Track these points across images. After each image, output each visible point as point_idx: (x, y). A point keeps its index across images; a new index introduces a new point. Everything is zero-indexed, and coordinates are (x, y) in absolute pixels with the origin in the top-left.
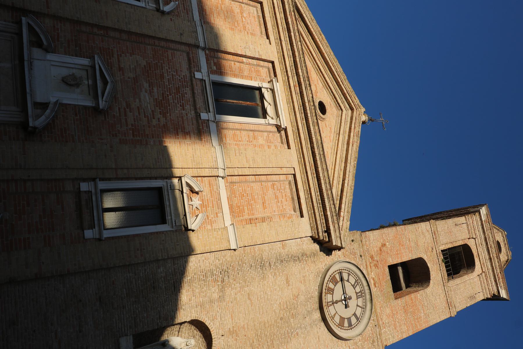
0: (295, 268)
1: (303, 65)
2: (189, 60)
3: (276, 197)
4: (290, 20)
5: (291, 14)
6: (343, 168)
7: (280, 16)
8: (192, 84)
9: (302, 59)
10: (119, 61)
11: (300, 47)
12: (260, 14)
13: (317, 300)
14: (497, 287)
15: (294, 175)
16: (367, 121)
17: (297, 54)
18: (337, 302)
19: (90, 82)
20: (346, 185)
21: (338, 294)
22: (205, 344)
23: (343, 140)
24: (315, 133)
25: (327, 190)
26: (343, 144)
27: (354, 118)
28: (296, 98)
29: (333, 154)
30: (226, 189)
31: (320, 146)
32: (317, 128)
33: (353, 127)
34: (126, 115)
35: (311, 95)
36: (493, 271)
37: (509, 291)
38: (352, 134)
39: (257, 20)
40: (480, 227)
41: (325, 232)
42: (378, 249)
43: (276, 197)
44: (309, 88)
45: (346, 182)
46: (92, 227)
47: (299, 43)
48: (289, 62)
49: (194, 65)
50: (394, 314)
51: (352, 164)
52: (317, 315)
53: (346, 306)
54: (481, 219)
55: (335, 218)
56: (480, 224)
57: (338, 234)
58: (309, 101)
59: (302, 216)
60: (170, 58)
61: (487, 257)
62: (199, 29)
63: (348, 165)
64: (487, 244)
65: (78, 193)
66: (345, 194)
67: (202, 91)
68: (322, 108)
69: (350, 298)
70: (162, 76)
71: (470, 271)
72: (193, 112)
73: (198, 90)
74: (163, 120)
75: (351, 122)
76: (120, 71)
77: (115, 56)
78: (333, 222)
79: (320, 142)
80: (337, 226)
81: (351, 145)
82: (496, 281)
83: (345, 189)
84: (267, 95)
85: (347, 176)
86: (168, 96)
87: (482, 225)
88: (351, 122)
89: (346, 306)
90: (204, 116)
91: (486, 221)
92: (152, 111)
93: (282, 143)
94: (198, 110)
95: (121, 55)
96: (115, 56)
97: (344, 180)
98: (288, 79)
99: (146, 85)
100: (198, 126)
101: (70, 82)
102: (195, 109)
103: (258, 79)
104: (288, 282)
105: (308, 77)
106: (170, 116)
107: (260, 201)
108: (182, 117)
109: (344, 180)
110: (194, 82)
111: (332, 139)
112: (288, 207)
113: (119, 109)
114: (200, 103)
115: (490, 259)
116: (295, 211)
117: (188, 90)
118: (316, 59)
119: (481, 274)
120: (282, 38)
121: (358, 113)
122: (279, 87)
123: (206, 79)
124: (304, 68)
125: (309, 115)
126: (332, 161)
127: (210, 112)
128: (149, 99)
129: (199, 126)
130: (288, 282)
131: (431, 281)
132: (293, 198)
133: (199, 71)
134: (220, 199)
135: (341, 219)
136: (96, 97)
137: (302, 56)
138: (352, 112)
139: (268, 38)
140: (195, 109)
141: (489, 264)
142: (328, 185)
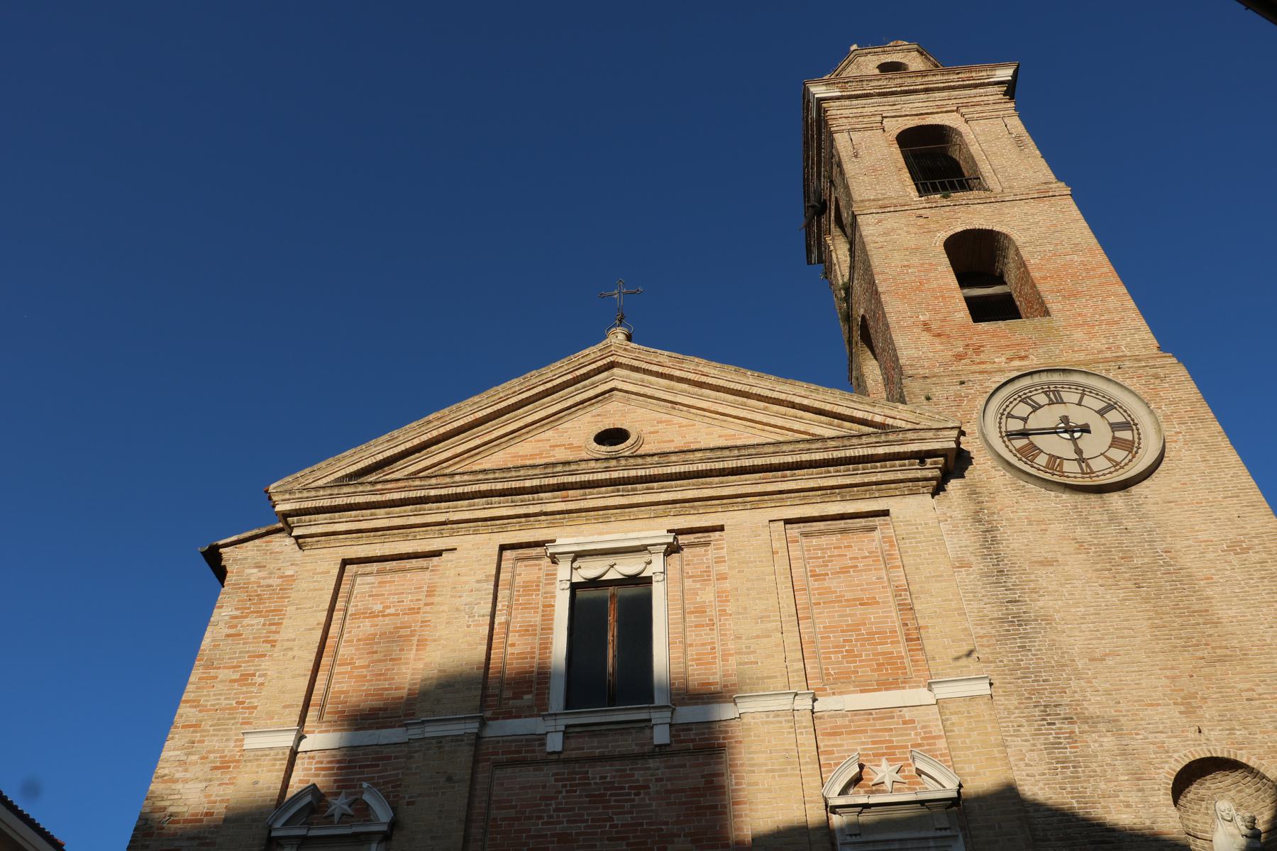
0: (1014, 542)
1: (514, 474)
2: (513, 763)
3: (844, 570)
4: (396, 496)
5: (381, 492)
6: (762, 404)
7: (382, 519)
8: (577, 760)
9: (497, 475)
11: (466, 477)
12: (375, 567)
13: (1080, 497)
14: (989, 84)
15: (788, 522)
17: (484, 487)
18: (1079, 451)
20: (806, 402)
21: (1058, 446)
22: (1219, 775)
23: (690, 395)
24: (685, 462)
25: (826, 449)
26: (700, 397)
27: (636, 363)
28: (595, 499)
29: (724, 424)
30: (841, 693)
31: (719, 454)
32: (673, 458)
33: (660, 369)
35: (592, 464)
36: (953, 88)
37: (998, 60)
38: (677, 373)
39: (388, 578)
40: (855, 102)
41: (922, 462)
42: (937, 340)
43: (844, 570)
44: (573, 467)
45: (798, 400)
47: (457, 478)
48: (502, 508)
49: (527, 752)
50: (1085, 323)
51: (751, 381)
52: (1115, 499)
53: (1085, 429)
54: (838, 98)
55: (891, 437)
56: (847, 102)
57: (930, 434)
58: (607, 469)
59: (885, 513)
60: (512, 813)
61: (922, 96)
62: (432, 731)
63: (754, 390)
64: (893, 93)
66: (828, 407)
67: (594, 734)
68: (613, 436)
69: (1065, 419)
71: (956, 139)
72: (652, 763)
73: (593, 746)
75: (646, 372)
78: (902, 442)
79: (709, 454)
80: (910, 435)
81: (704, 379)
82: (976, 86)
83: (817, 405)
84: (590, 570)
85: (783, 397)
86: (616, 826)
87: (850, 97)
88: (646, 372)
89: (1085, 429)
90: (661, 736)
91: (843, 89)
93: (707, 544)
94: (646, 749)
97: (793, 405)
98: (546, 514)
102: (643, 756)
103: (549, 588)
104: (1046, 563)
105: (546, 465)
106: (666, 823)
107: (859, 610)
108: (667, 791)
109: (793, 405)
110: (574, 754)
111: (685, 422)
112: (864, 544)
114: (628, 744)
115: (926, 90)
116: (873, 529)
118: (486, 438)
119: (963, 115)
120: (442, 518)
121: (621, 352)
122: (568, 538)
123: (562, 723)
124: (522, 473)
125: (641, 473)
126: (742, 428)
127: (650, 720)
130: (1046, 563)
131: (997, 229)
132: (843, 531)
133: (541, 739)
134: (868, 712)
135: (889, 421)
137: (491, 476)
138: (620, 365)
139: (438, 553)
140: (643, 756)
141: (937, 95)
142: (814, 446)
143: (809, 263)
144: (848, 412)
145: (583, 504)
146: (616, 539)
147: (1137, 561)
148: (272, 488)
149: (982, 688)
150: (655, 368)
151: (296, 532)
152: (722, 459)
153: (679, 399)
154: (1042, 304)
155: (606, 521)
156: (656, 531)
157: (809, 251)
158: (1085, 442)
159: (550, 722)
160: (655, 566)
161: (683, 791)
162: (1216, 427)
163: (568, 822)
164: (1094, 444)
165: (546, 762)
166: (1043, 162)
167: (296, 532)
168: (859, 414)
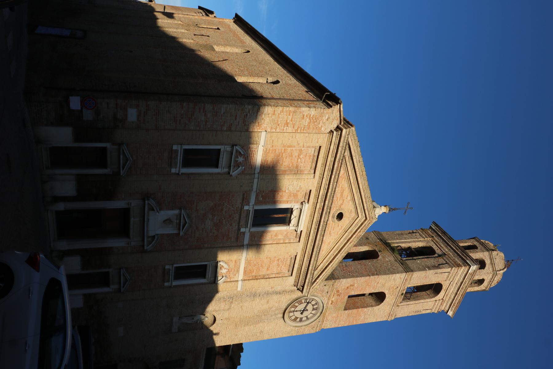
0: (275, 297)
2: (243, 198)
3: (278, 265)
4: (336, 166)
5: (339, 161)
6: (335, 254)
13: (284, 310)
16: (387, 212)
17: (330, 190)
18: (296, 311)
20: (330, 266)
21: (301, 307)
23: (347, 236)
26: (345, 239)
28: (317, 215)
35: (327, 219)
37: (456, 314)
38: (354, 236)
40: (464, 275)
42: (346, 287)
43: (278, 265)
45: (331, 264)
46: (168, 281)
47: (335, 184)
50: (338, 316)
51: (343, 254)
52: (282, 315)
53: (302, 313)
54: (468, 271)
56: (465, 273)
58: (324, 222)
61: (455, 292)
62: (256, 181)
63: (339, 254)
64: (461, 285)
65: (164, 269)
66: (326, 270)
67: (247, 216)
68: (340, 216)
69: (307, 310)
70: (222, 210)
71: (432, 295)
72: (237, 227)
73: (243, 215)
80: (309, 287)
81: (349, 242)
82: (450, 305)
83: (328, 268)
84: (295, 213)
85: (334, 261)
90: (242, 230)
91: (470, 274)
93: (296, 237)
97: (331, 262)
99: (210, 216)
100: (238, 234)
101: (168, 221)
102: (239, 225)
103: (293, 202)
104: (268, 302)
105: (331, 208)
107: (266, 267)
109: (331, 262)
110: (243, 212)
114: (243, 222)
115: (456, 294)
117: (237, 217)
119: (439, 300)
120: (325, 176)
122: (307, 208)
123: (251, 210)
125: (320, 229)
129: (238, 234)
130: (268, 302)
135: (316, 283)
136: (179, 229)
139: (314, 173)
140: (239, 225)
143: (434, 223)
144: (323, 274)
145: (317, 212)
146: (303, 219)
147: (263, 317)
148: (353, 128)
149: (239, 289)
150: (359, 230)
151: (335, 133)
152: (317, 248)
154: (349, 309)
155: (311, 216)
156: (303, 226)
157: (436, 225)
158: (300, 313)
159: (252, 207)
160: (292, 227)
162: (294, 335)
164: (298, 314)
165: (242, 205)
166: (406, 315)
167: (335, 133)
168: (321, 277)
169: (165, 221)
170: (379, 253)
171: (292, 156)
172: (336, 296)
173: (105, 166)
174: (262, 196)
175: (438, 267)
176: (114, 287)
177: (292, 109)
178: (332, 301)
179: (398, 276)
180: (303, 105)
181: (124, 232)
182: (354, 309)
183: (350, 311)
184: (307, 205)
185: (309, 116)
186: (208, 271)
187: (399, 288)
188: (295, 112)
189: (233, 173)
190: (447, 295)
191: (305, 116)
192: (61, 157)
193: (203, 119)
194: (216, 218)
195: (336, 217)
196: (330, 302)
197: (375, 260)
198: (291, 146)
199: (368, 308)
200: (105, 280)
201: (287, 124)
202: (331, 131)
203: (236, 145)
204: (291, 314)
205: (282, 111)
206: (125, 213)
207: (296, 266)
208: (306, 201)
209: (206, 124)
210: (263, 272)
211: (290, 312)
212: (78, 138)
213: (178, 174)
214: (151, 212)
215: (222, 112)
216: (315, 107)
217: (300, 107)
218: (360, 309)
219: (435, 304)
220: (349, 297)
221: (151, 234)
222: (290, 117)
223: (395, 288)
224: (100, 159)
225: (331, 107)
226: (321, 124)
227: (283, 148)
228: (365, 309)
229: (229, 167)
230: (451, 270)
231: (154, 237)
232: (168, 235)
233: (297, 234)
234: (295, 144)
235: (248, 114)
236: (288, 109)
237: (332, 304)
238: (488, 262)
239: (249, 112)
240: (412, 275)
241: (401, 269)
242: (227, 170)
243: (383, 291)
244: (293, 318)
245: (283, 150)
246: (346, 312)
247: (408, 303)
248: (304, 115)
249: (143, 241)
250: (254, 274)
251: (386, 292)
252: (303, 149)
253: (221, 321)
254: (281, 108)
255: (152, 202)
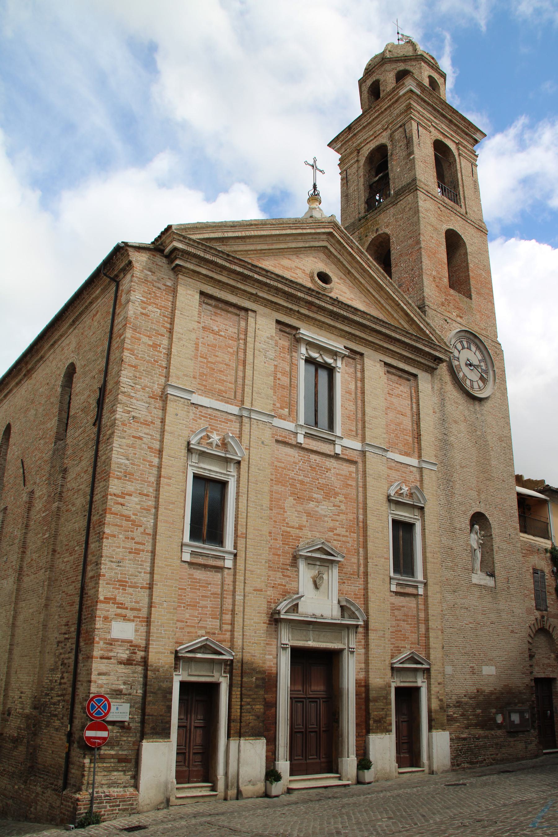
1: (294, 285)
10: (293, 527)
12: (213, 302)
19: (318, 563)
23: (358, 272)
25: (411, 339)
29: (366, 295)
30: (394, 452)
34: (339, 535)
41: (435, 360)
46: (416, 587)
49: (289, 439)
60: (282, 465)
68: (324, 278)
70: (302, 482)
74: (341, 498)
76: (302, 529)
77: (288, 529)
80: (438, 348)
86: (319, 483)
92: (334, 506)
95: (287, 523)
96: (288, 529)
99: (312, 505)
106: (336, 487)
108: (337, 474)
113: (334, 540)
116: (409, 380)
122: (307, 332)
126: (373, 302)
127: (334, 441)
128: (324, 505)
130: (456, 422)
131: (462, 236)
132: (400, 377)
136: (332, 562)
142: (408, 335)
145: (315, 316)
147: (478, 433)
151: (178, 262)
153: (353, 271)
154: (469, 290)
161: (342, 475)
163: (304, 476)
169: (316, 587)
170: (380, 232)
171: (214, 346)
172: (449, 309)
173: (215, 686)
174: (282, 408)
175: (409, 142)
176: (421, 682)
177: (129, 333)
178: (457, 316)
179: (421, 203)
180: (123, 313)
181: (330, 660)
182: (469, 284)
183: (473, 290)
184: (302, 331)
185: (145, 305)
186: (402, 519)
187: (440, 205)
188: (135, 329)
189: (239, 455)
190: (452, 136)
191: (144, 311)
192: (197, 762)
193: (136, 499)
194: (315, 496)
195: (324, 285)
196: (459, 319)
197: (393, 239)
198: (197, 344)
199: (469, 261)
200: (408, 697)
201: (155, 346)
202: (173, 269)
203: (189, 443)
204: (476, 386)
205: (132, 351)
206: (299, 655)
207: (401, 365)
208: (294, 332)
209: (148, 496)
210: (407, 423)
211: (472, 387)
212: (163, 732)
213: (235, 555)
214: (300, 609)
215: (127, 462)
216: (129, 292)
217: (126, 318)
218: (471, 274)
219: (464, 157)
220: (452, 286)
221: (336, 612)
222: (145, 339)
223: (439, 212)
224: (200, 696)
225: (130, 262)
226: (160, 285)
227: (199, 359)
228: (471, 266)
229: (227, 461)
230: (415, 121)
231: (342, 607)
232: (342, 582)
233: (348, 357)
234: (193, 336)
235: (133, 414)
236: (127, 341)
237: (461, 317)
238: (401, 66)
239: (129, 412)
240: (422, 182)
241: (410, 198)
242: (232, 465)
243: (444, 232)
244: (481, 384)
245: (203, 360)
246: (474, 296)
247: (462, 197)
248: (142, 314)
249: (348, 627)
250: (410, 439)
251: (445, 227)
252: (202, 325)
253: (482, 505)
254: (126, 353)
255: (283, 607)
